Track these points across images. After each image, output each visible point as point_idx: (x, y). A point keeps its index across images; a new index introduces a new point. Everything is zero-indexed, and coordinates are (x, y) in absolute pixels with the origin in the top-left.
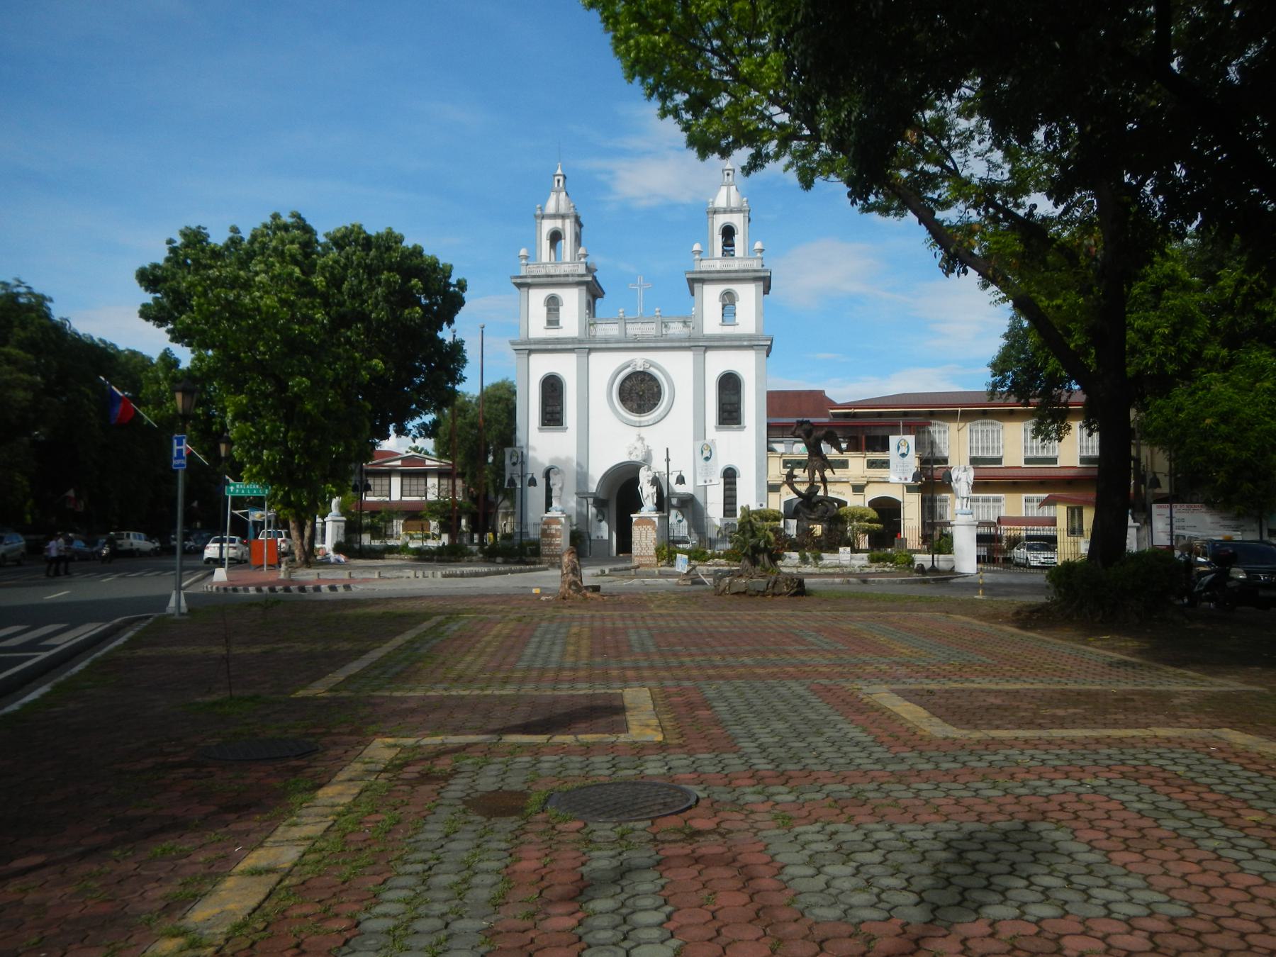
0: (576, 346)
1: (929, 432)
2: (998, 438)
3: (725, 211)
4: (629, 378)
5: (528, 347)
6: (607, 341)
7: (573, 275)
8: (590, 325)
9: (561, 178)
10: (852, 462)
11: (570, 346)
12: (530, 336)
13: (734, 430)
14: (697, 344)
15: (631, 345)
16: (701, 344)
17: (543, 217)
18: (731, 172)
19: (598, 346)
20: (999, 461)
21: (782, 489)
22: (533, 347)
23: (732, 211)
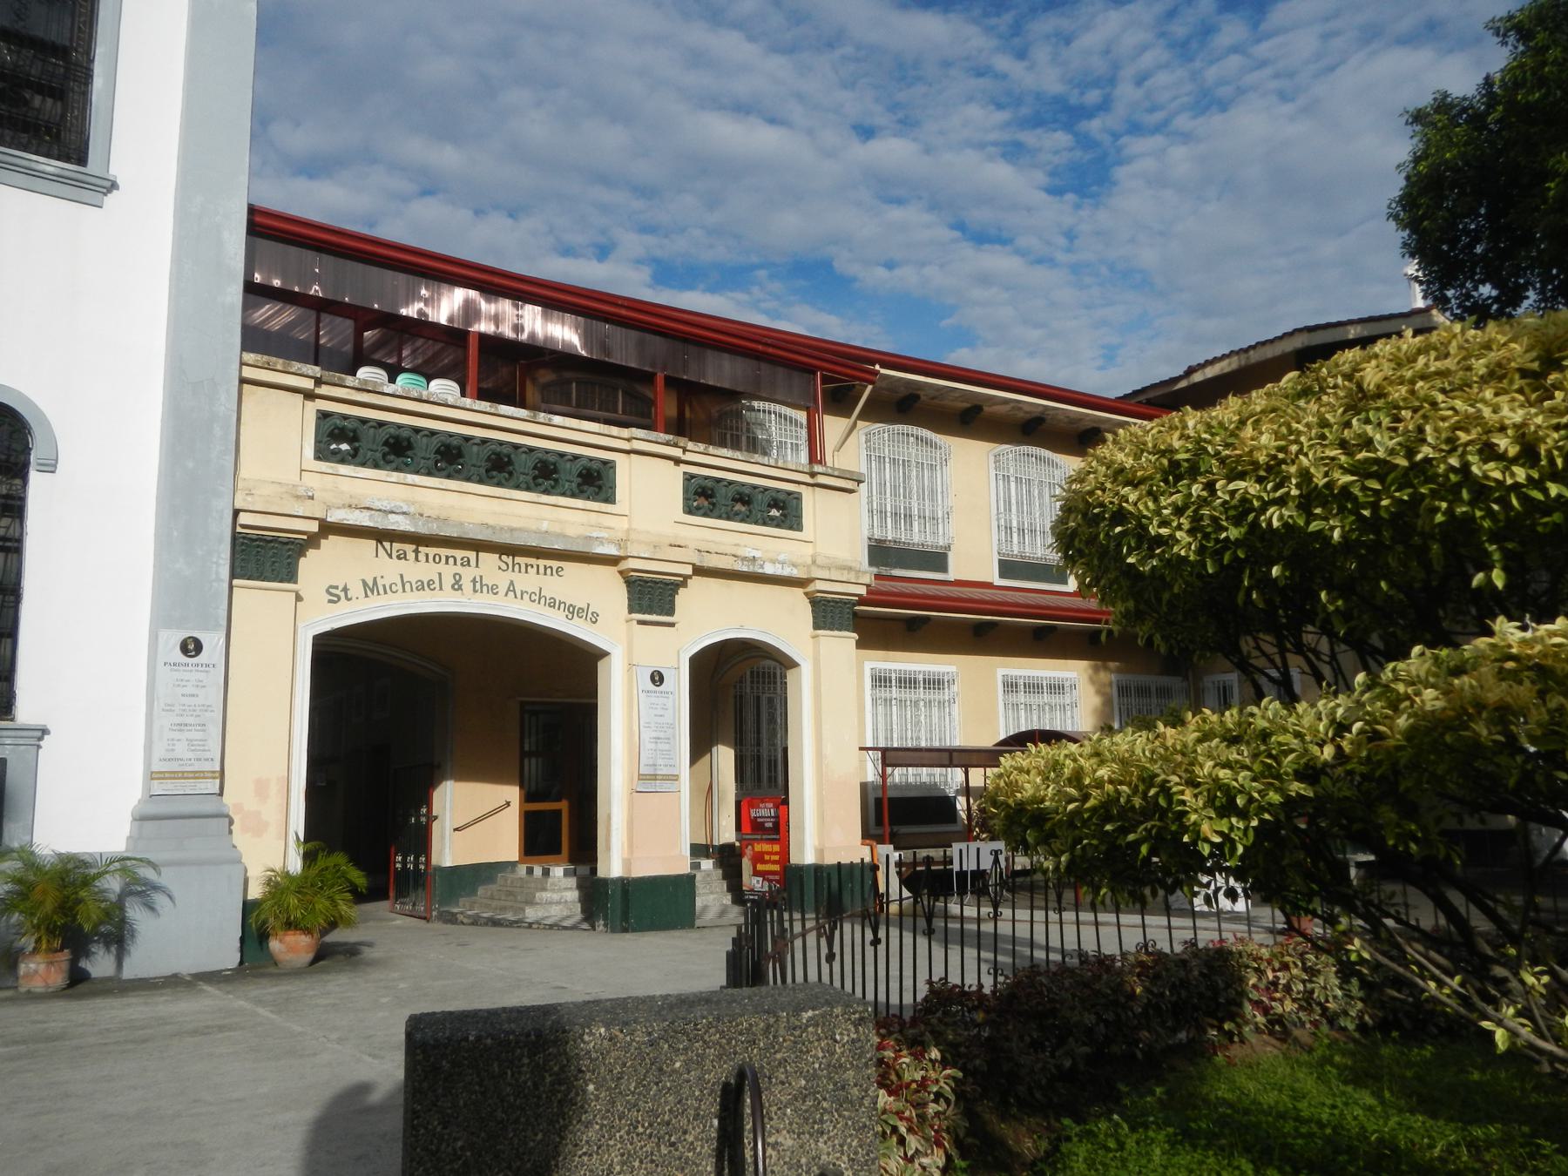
2: (933, 492)
20: (937, 560)
21: (308, 565)
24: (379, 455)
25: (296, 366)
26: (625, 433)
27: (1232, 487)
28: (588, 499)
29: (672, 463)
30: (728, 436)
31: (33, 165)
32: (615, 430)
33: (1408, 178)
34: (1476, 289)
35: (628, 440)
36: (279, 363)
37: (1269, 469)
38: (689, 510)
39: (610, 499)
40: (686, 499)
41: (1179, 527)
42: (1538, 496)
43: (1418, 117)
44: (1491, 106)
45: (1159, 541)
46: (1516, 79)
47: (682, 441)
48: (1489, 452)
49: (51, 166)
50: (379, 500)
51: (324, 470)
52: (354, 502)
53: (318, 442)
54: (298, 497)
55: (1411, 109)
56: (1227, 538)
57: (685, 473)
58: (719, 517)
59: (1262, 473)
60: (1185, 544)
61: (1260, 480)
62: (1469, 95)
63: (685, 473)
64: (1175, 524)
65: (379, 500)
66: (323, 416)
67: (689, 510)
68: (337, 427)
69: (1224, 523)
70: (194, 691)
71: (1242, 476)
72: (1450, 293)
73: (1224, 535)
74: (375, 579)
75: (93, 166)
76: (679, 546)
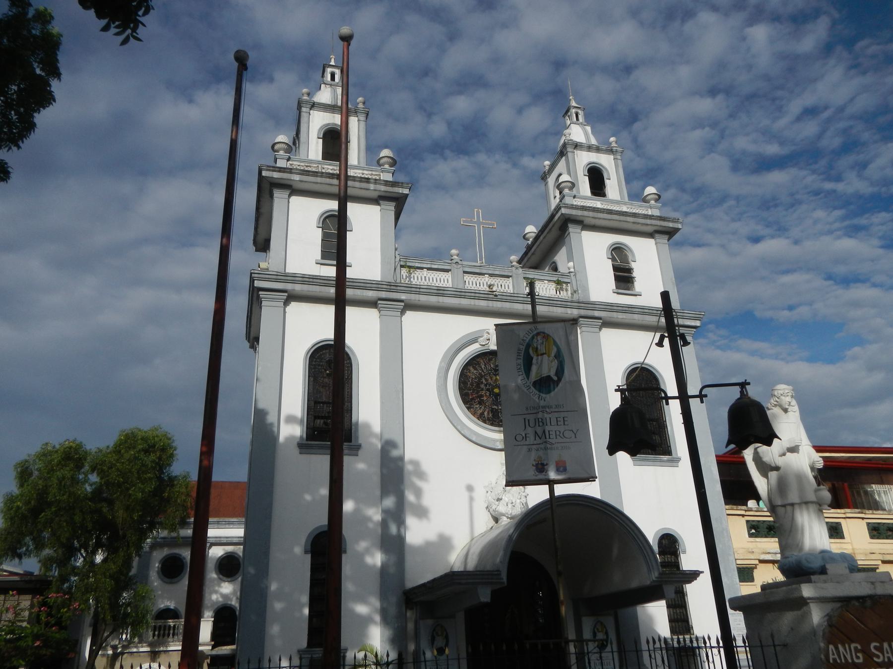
0: (384, 295)
1: (866, 493)
3: (590, 148)
4: (473, 362)
5: (289, 286)
6: (440, 292)
7: (376, 181)
8: (402, 266)
9: (337, 72)
10: (846, 526)
11: (371, 294)
12: (287, 271)
13: (662, 463)
14: (590, 313)
15: (482, 304)
16: (597, 314)
17: (313, 106)
18: (580, 111)
19: (423, 299)
22: (298, 288)
23: (598, 150)
24: (766, 533)
25: (740, 507)
26: (842, 511)
28: (834, 538)
29: (861, 520)
30: (854, 492)
31: (662, 459)
32: (839, 511)
35: (844, 513)
36: (735, 507)
38: (872, 537)
39: (842, 537)
40: (869, 533)
47: (864, 511)
49: (665, 458)
50: (771, 549)
51: (753, 541)
52: (765, 552)
53: (748, 531)
54: (750, 552)
57: (866, 523)
58: (883, 539)
63: (866, 523)
65: (771, 549)
66: (747, 522)
67: (872, 537)
68: (752, 525)
70: (739, 623)
74: (775, 578)
75: (674, 455)
76: (874, 553)
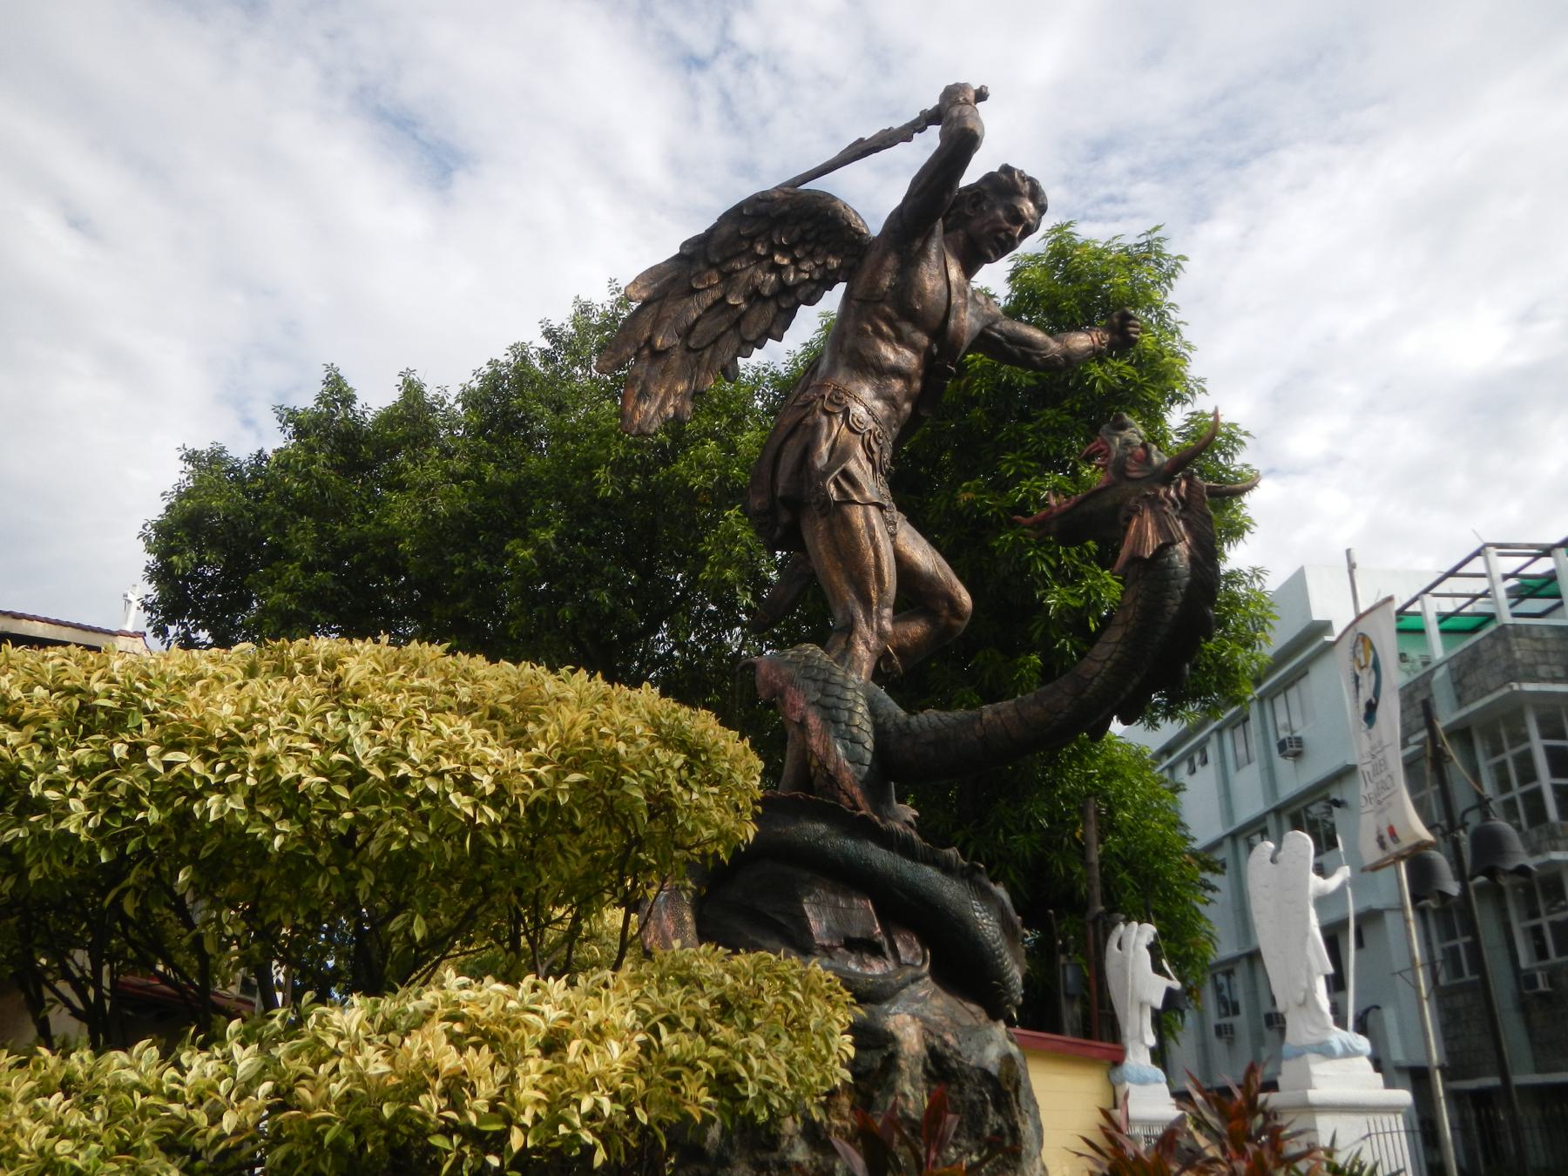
27: (169, 757)
33: (168, 508)
34: (196, 631)
37: (221, 744)
41: (75, 794)
42: (491, 840)
43: (192, 457)
44: (254, 477)
45: (40, 805)
46: (284, 461)
48: (465, 784)
55: (189, 447)
56: (144, 820)
59: (214, 749)
60: (78, 819)
61: (206, 757)
62: (242, 460)
64: (70, 788)
69: (144, 800)
71: (180, 747)
72: (172, 629)
73: (141, 815)
